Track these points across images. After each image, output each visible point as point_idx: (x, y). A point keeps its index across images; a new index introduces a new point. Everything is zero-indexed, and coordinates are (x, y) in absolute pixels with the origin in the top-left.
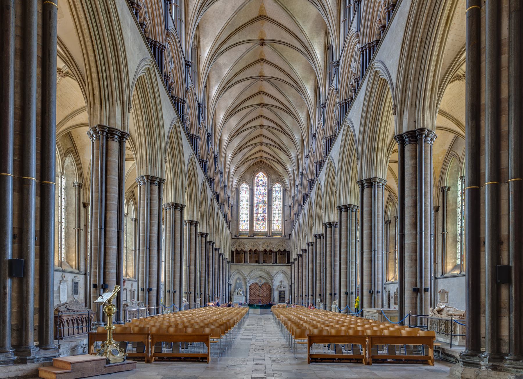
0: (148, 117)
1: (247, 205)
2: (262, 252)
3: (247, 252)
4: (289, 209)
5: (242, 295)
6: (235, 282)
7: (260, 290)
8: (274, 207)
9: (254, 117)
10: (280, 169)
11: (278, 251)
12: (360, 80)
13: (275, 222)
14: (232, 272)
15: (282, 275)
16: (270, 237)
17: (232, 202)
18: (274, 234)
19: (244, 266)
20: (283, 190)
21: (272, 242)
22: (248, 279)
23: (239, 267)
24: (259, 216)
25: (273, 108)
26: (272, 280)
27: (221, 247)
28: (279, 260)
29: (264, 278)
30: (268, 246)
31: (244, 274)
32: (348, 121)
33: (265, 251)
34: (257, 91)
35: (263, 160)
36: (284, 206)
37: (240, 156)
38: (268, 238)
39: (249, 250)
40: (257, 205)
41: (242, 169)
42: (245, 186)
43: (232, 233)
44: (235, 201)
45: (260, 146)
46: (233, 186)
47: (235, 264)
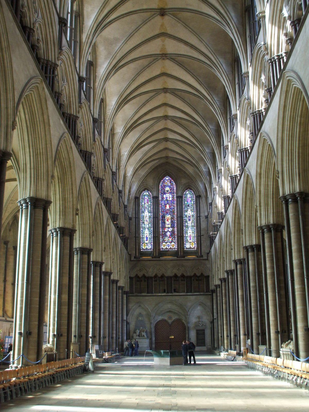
1: (150, 217)
3: (151, 278)
4: (205, 220)
10: (190, 170)
13: (189, 239)
14: (130, 305)
15: (199, 308)
17: (130, 213)
19: (147, 298)
20: (196, 197)
24: (166, 230)
29: (175, 313)
36: (198, 218)
37: (139, 155)
40: (163, 217)
41: (142, 173)
42: (147, 193)
43: (130, 253)
44: (134, 212)
46: (132, 192)
47: (134, 295)
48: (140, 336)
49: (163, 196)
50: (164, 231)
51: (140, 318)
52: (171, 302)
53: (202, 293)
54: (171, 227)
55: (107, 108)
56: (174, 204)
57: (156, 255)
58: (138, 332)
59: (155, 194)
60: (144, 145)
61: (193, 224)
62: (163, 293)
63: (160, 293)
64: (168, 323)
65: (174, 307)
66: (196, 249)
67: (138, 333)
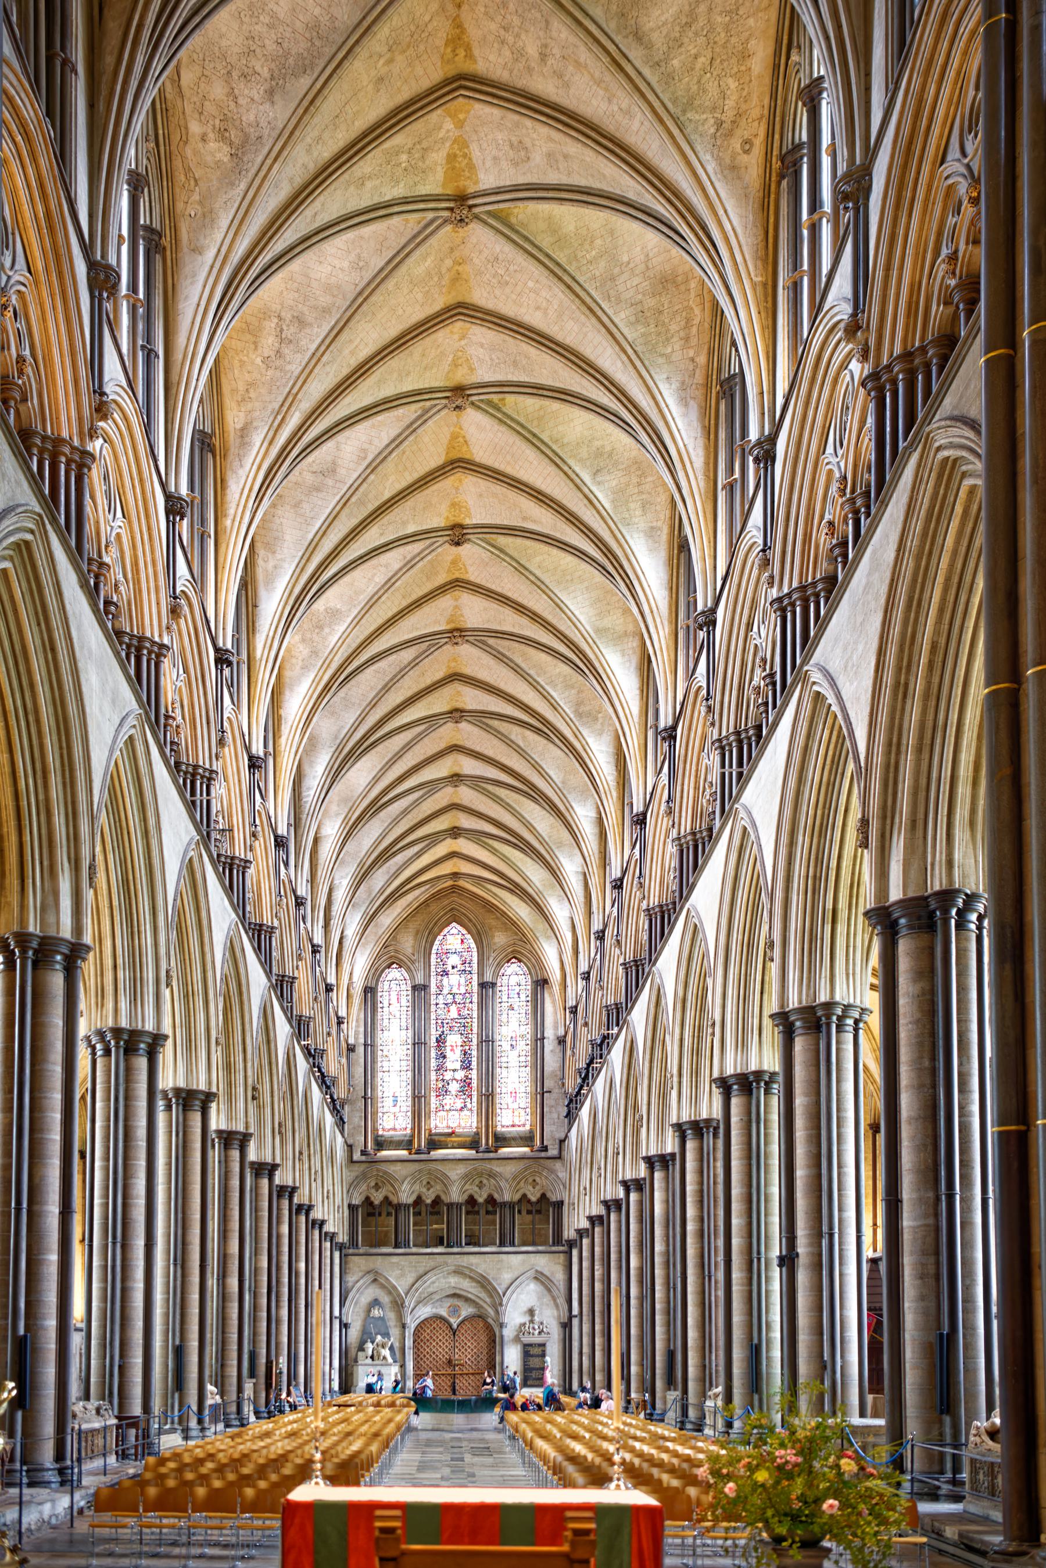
0: (123, 862)
2: (459, 1206)
3: (407, 1206)
5: (390, 1360)
6: (362, 1315)
7: (455, 1341)
8: (503, 1044)
9: (430, 753)
11: (520, 1201)
12: (767, 712)
14: (350, 1279)
15: (533, 1287)
16: (488, 1151)
18: (501, 1140)
19: (395, 1259)
21: (498, 1169)
22: (410, 1302)
23: (378, 1263)
25: (495, 723)
26: (498, 1305)
27: (317, 1200)
28: (523, 1232)
29: (467, 1300)
30: (481, 1186)
31: (394, 1287)
32: (742, 814)
33: (471, 1201)
34: (439, 675)
35: (462, 883)
38: (480, 1155)
39: (410, 1201)
40: (441, 1041)
41: (388, 919)
45: (449, 841)
46: (355, 979)
47: (361, 1251)
48: (376, 1357)
49: (441, 981)
50: (443, 1080)
51: (376, 1312)
52: (458, 1272)
53: (540, 1248)
54: (463, 1068)
55: (303, 784)
56: (471, 1002)
57: (419, 1145)
58: (369, 1347)
59: (420, 979)
60: (394, 854)
61: (523, 1059)
62: (436, 1246)
63: (427, 1247)
64: (451, 1326)
65: (467, 1286)
66: (528, 1127)
67: (370, 1353)
